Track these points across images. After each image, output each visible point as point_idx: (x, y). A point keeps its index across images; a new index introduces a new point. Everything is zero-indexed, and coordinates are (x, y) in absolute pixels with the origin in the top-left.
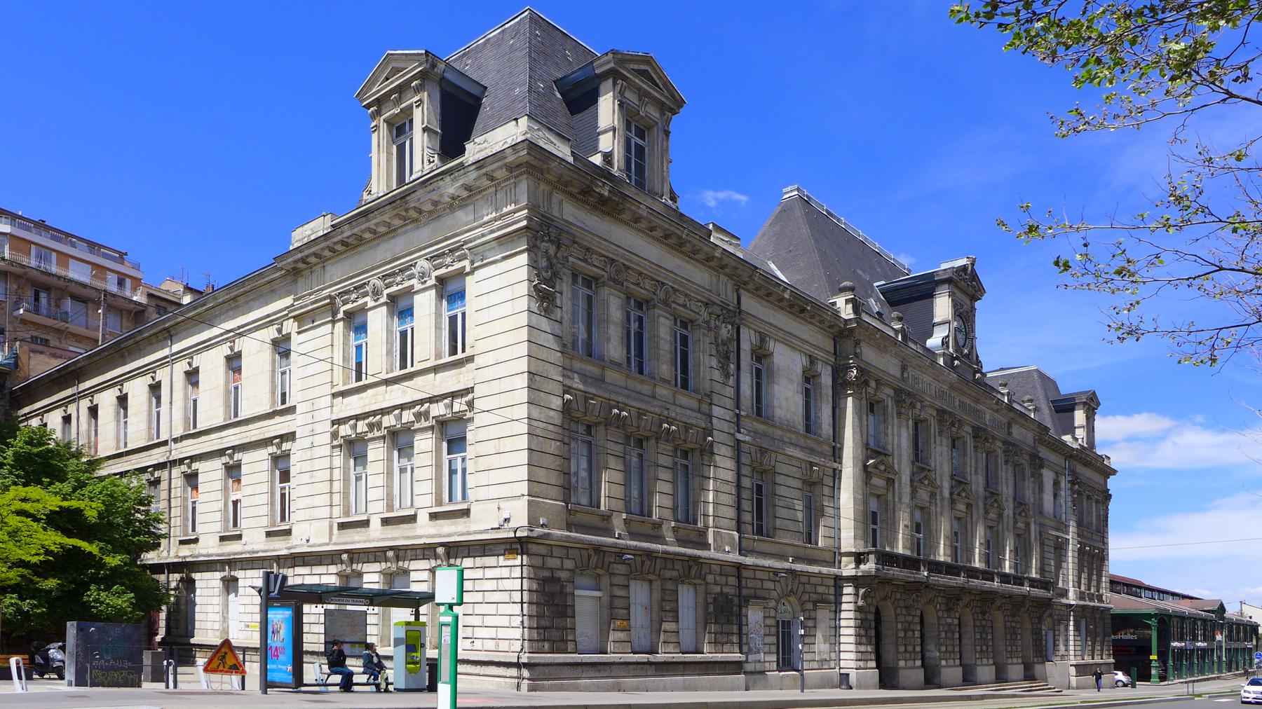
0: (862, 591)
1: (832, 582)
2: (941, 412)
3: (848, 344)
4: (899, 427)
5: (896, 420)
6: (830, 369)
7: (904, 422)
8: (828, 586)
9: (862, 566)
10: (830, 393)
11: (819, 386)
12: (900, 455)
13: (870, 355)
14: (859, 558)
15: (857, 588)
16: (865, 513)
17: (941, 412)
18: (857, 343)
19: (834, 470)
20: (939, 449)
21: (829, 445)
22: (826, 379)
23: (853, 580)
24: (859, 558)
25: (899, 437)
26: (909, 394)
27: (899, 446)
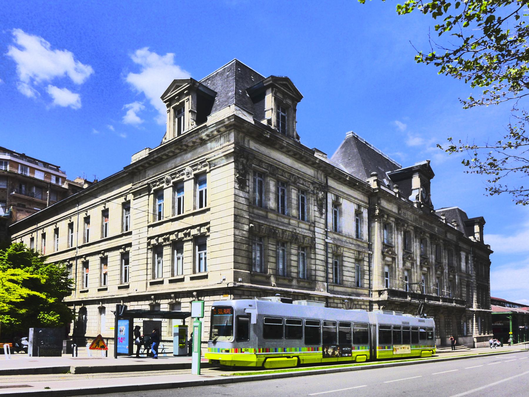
0: (381, 307)
1: (368, 304)
2: (416, 228)
3: (375, 199)
4: (397, 234)
5: (396, 232)
6: (367, 210)
7: (400, 233)
8: (367, 306)
9: (381, 296)
10: (367, 221)
11: (362, 218)
12: (398, 247)
13: (384, 204)
14: (380, 293)
15: (379, 306)
16: (383, 273)
17: (416, 228)
18: (379, 199)
19: (369, 254)
20: (415, 244)
21: (367, 243)
22: (365, 214)
23: (379, 303)
24: (380, 293)
25: (398, 239)
26: (402, 220)
27: (397, 243)
